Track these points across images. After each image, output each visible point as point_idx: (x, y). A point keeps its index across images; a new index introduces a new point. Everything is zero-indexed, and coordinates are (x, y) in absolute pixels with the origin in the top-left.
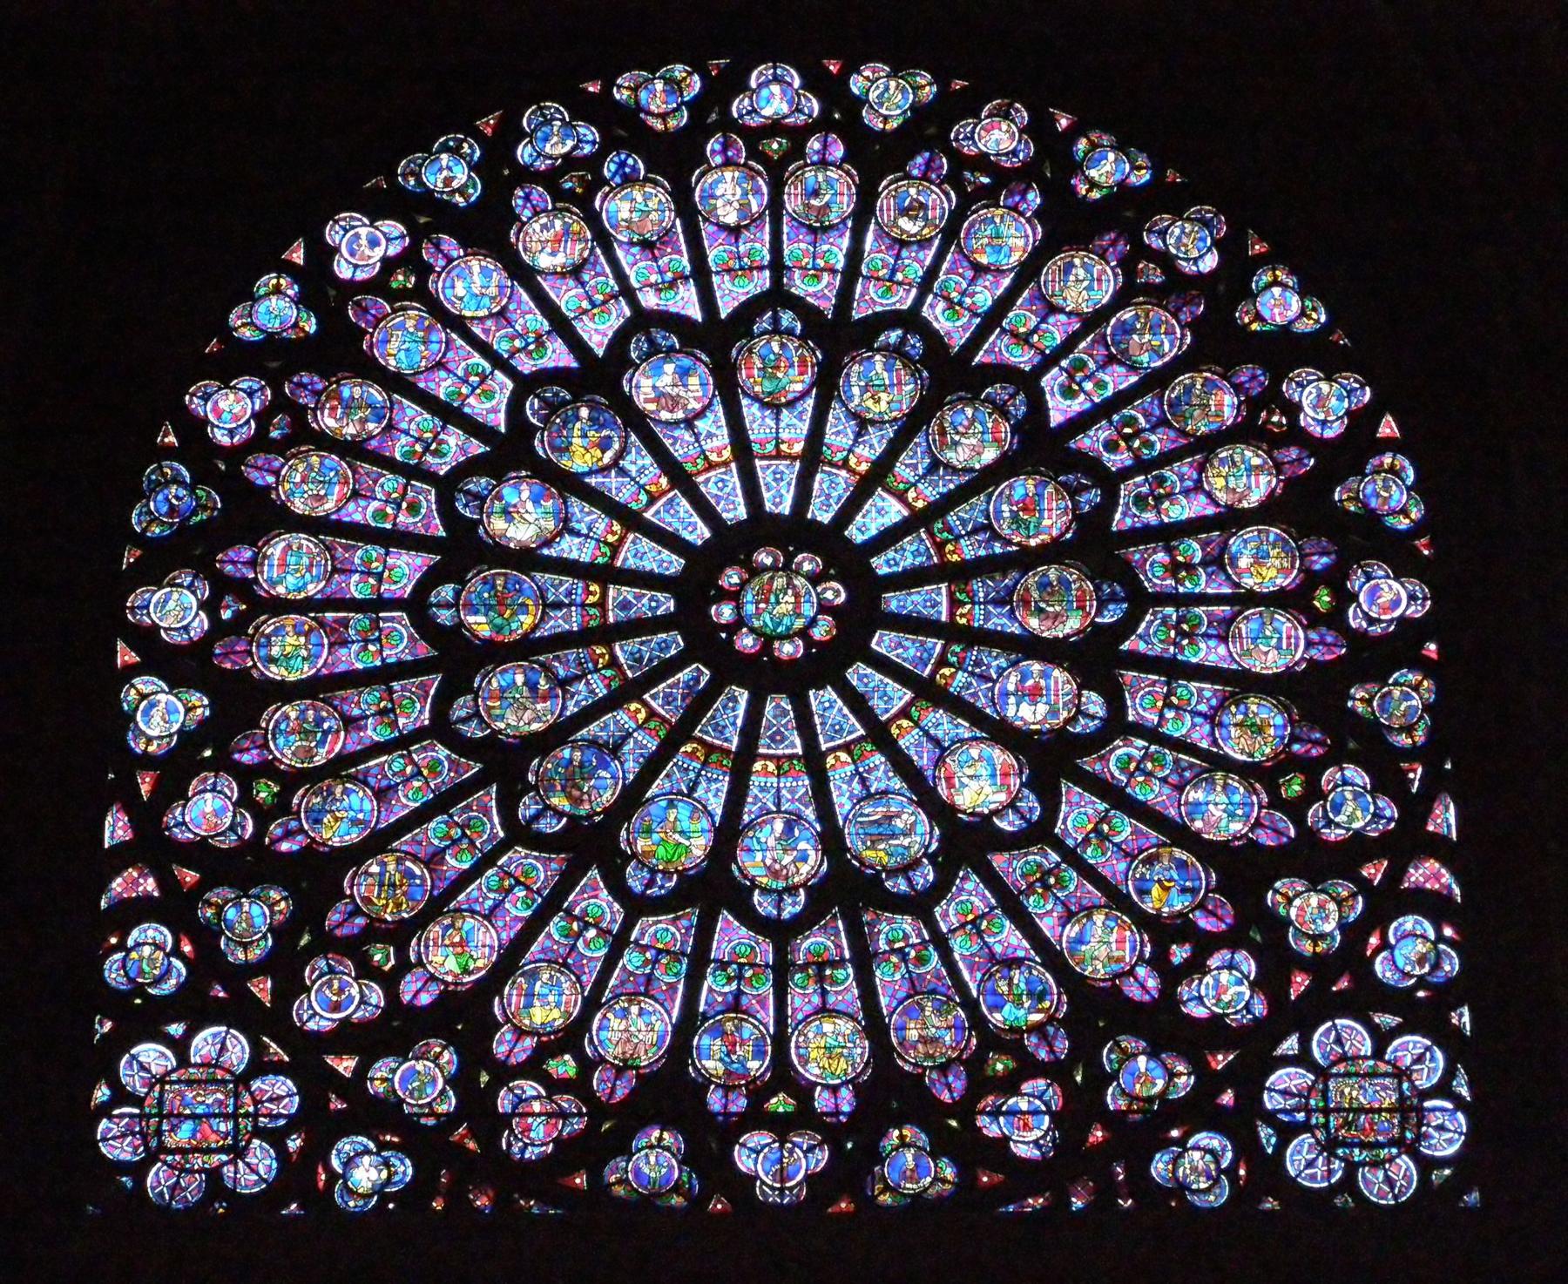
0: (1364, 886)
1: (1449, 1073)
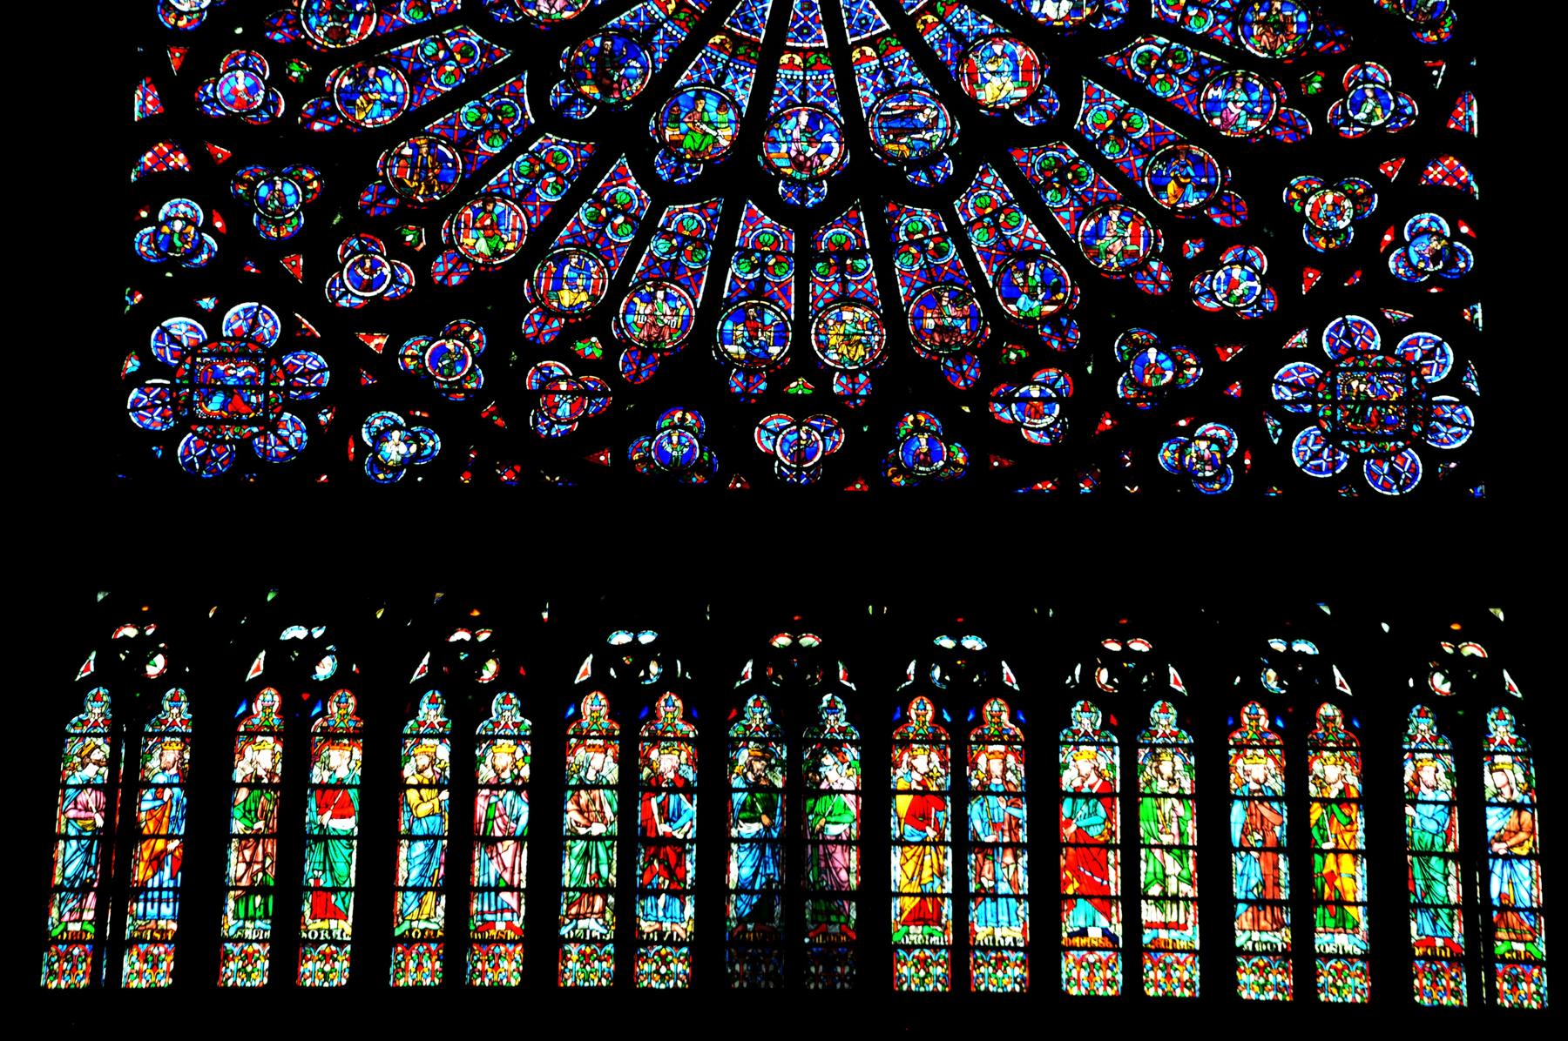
0: (1381, 183)
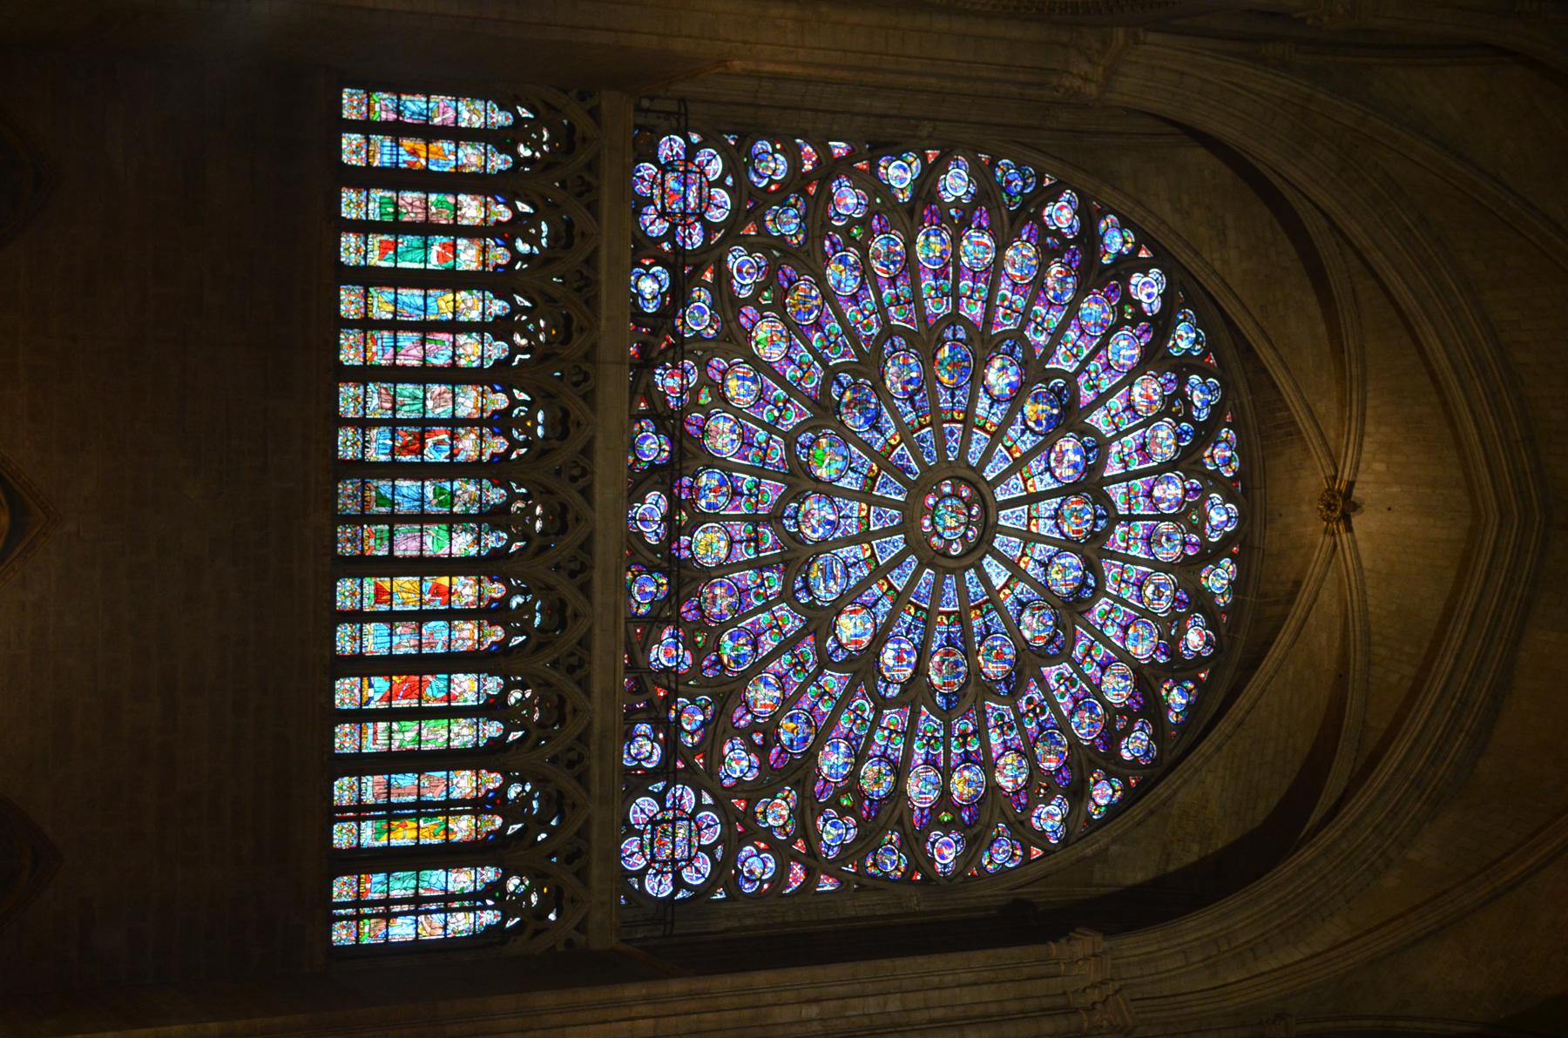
0: (792, 840)
1: (689, 887)
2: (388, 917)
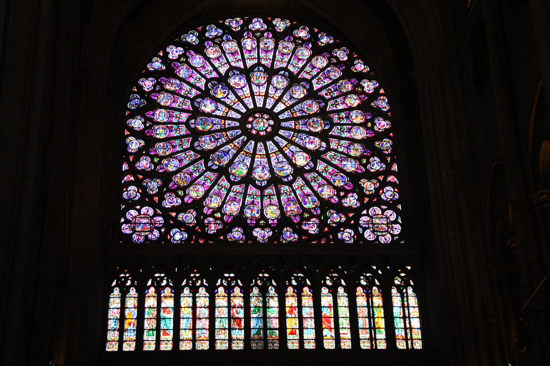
1: (397, 218)
2: (411, 328)
